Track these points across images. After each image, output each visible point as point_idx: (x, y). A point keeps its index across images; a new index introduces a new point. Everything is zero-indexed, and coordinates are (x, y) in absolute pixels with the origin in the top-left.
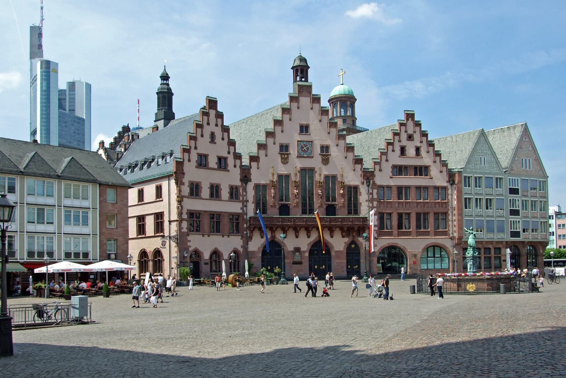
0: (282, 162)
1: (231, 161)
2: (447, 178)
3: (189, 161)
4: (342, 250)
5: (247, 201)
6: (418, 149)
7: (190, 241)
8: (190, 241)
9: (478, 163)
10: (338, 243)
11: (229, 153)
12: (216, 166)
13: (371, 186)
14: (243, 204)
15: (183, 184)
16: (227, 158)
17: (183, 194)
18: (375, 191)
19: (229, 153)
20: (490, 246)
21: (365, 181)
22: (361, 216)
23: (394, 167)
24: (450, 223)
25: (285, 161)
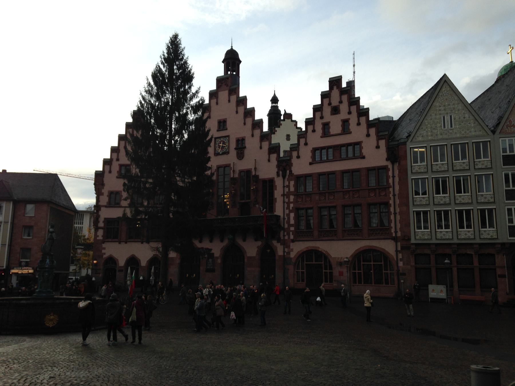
2: (385, 156)
3: (110, 172)
4: (254, 255)
6: (345, 123)
7: (104, 249)
8: (104, 249)
9: (438, 125)
13: (287, 177)
15: (102, 194)
17: (100, 204)
18: (292, 183)
20: (469, 252)
21: (281, 172)
22: (275, 213)
23: (314, 150)
24: (392, 217)
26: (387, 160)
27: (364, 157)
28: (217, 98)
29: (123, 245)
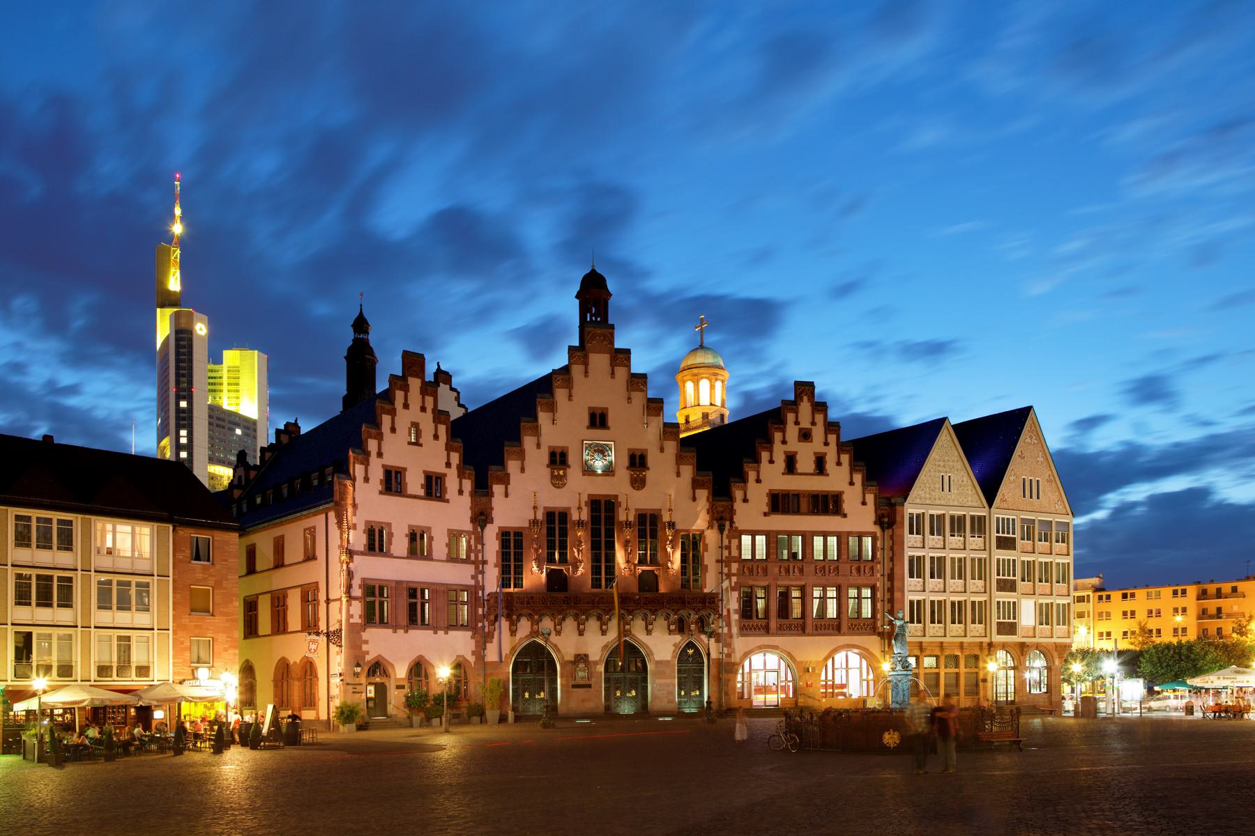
0: (554, 485)
1: (452, 482)
2: (872, 517)
5: (485, 562)
7: (366, 642)
8: (366, 642)
10: (661, 645)
11: (448, 465)
12: (422, 492)
13: (726, 532)
14: (477, 568)
16: (445, 475)
19: (448, 465)
25: (558, 482)
26: (875, 523)
27: (845, 516)
28: (586, 364)
29: (401, 632)
